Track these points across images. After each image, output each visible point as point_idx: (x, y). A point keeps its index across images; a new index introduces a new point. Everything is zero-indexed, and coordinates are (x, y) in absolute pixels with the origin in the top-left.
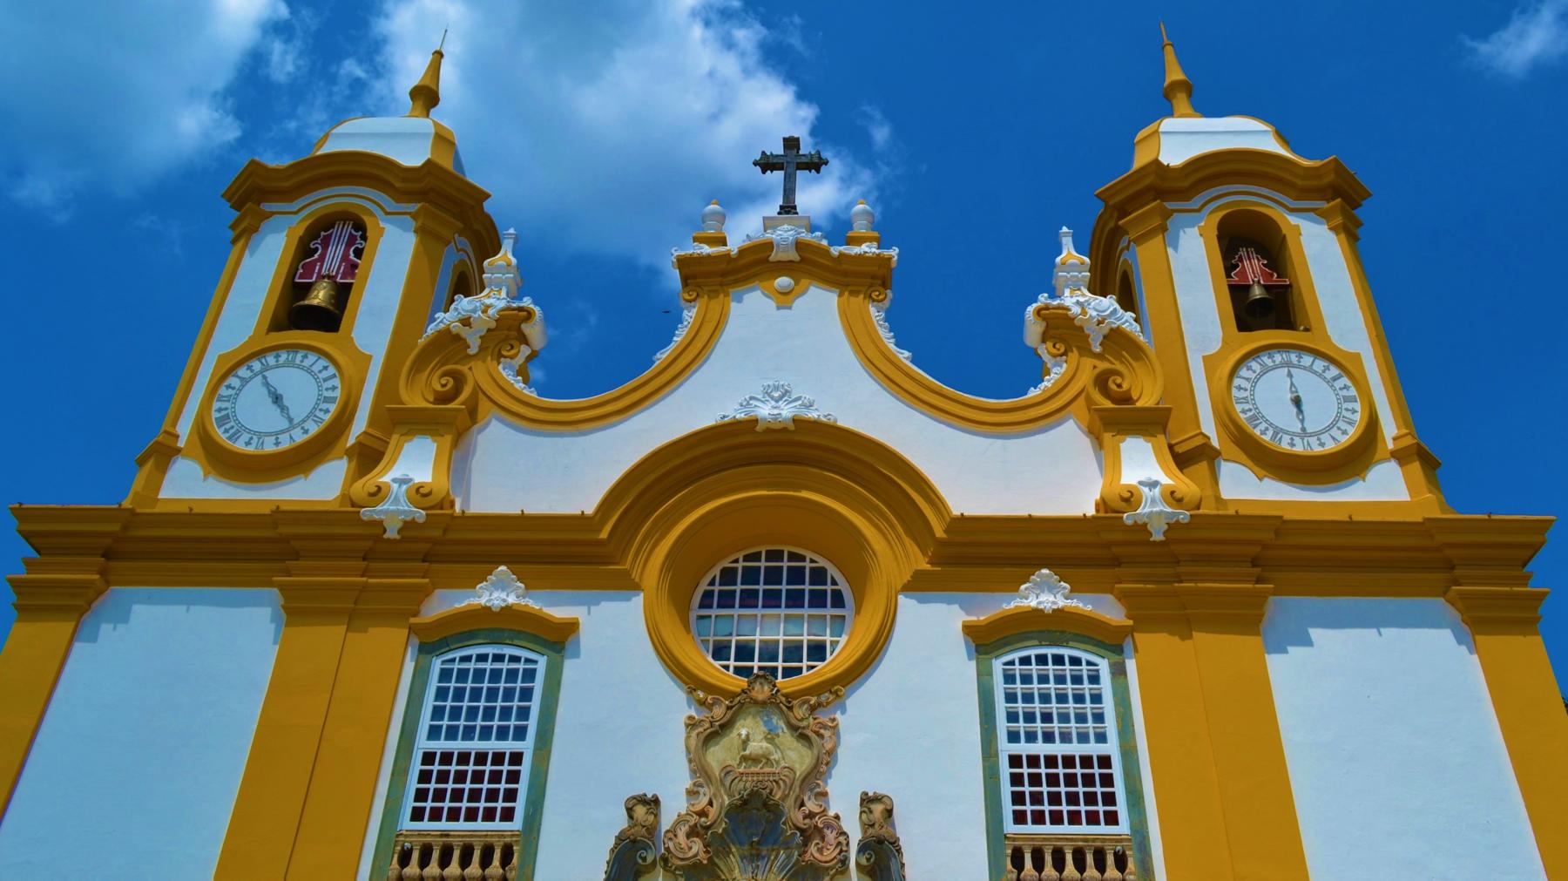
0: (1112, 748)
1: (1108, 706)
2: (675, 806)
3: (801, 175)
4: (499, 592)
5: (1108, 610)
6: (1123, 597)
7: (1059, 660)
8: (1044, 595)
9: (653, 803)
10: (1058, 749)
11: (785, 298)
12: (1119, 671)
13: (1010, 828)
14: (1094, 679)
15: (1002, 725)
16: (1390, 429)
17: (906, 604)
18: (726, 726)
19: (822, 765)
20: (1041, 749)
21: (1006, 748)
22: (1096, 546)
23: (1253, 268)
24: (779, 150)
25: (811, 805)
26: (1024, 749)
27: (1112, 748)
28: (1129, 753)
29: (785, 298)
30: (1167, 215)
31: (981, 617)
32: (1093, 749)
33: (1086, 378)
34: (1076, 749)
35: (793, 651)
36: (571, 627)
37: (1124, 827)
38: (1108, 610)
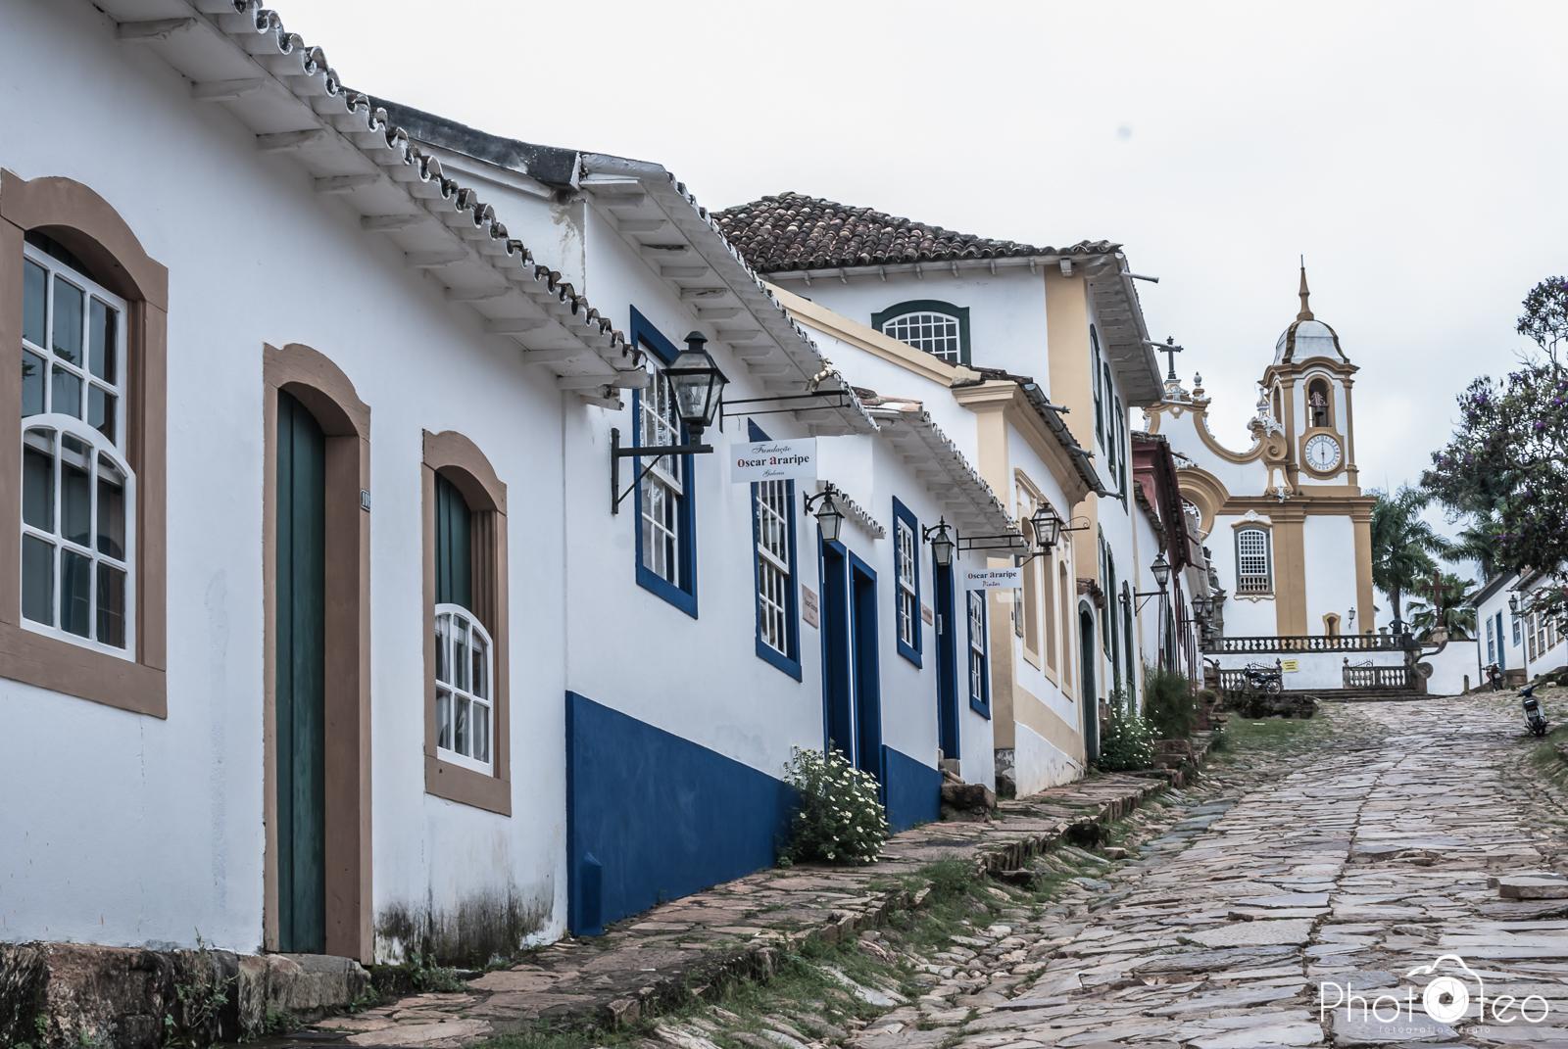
0: (1265, 555)
1: (1265, 545)
3: (1175, 353)
5: (1266, 519)
6: (1272, 517)
8: (1251, 516)
10: (1253, 555)
11: (1177, 415)
12: (1268, 536)
16: (1347, 462)
17: (1217, 517)
20: (1248, 555)
21: (1241, 556)
22: (1267, 502)
23: (1318, 396)
24: (1166, 343)
26: (1245, 556)
29: (1177, 415)
30: (1294, 380)
31: (1235, 522)
32: (1261, 555)
33: (1266, 447)
34: (1257, 555)
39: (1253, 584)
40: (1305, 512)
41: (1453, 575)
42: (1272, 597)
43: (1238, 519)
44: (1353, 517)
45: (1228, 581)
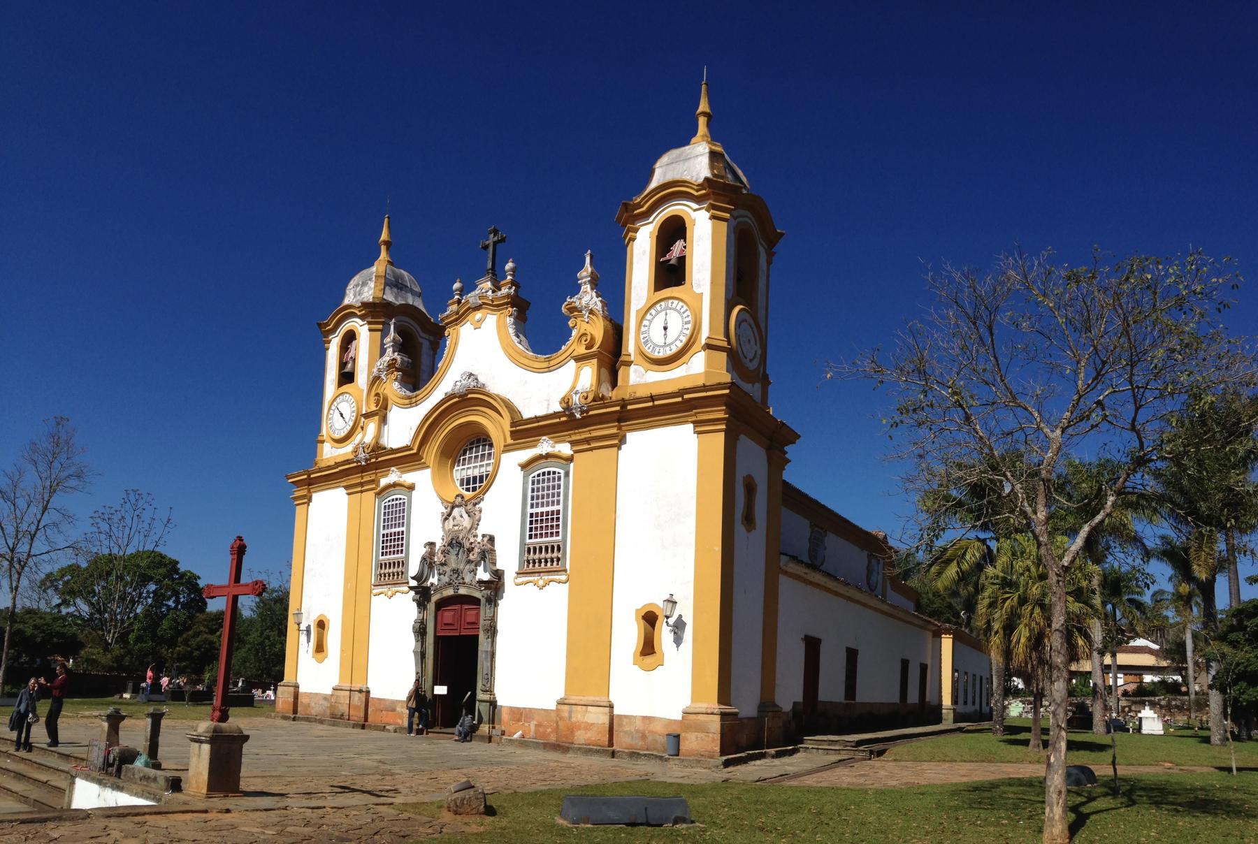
0: (560, 507)
2: (439, 544)
4: (393, 476)
6: (573, 443)
7: (549, 473)
8: (545, 446)
9: (432, 544)
10: (545, 509)
12: (567, 474)
13: (528, 541)
14: (559, 479)
15: (529, 501)
18: (449, 515)
19: (475, 525)
20: (540, 510)
25: (472, 540)
26: (534, 511)
27: (560, 507)
28: (565, 507)
32: (555, 508)
34: (550, 509)
35: (481, 477)
36: (411, 488)
37: (559, 538)
38: (565, 449)
39: (542, 558)
40: (619, 428)
41: (177, 563)
42: (564, 578)
43: (526, 455)
44: (697, 423)
45: (508, 558)
